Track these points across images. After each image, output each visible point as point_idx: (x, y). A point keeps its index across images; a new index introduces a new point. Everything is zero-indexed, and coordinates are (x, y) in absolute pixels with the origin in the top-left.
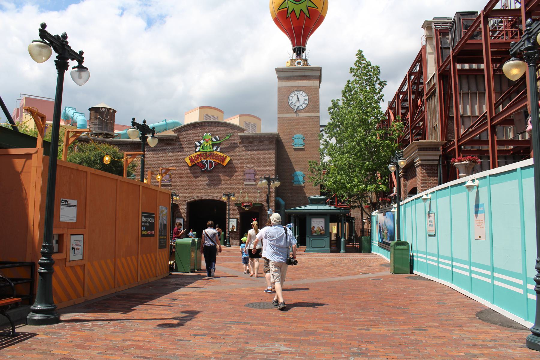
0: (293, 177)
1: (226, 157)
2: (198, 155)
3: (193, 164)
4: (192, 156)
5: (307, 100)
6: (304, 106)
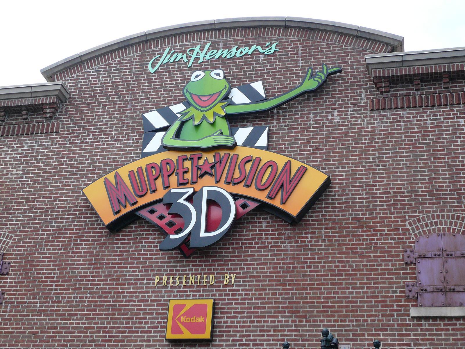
1: (302, 172)
2: (152, 166)
3: (124, 211)
4: (124, 172)
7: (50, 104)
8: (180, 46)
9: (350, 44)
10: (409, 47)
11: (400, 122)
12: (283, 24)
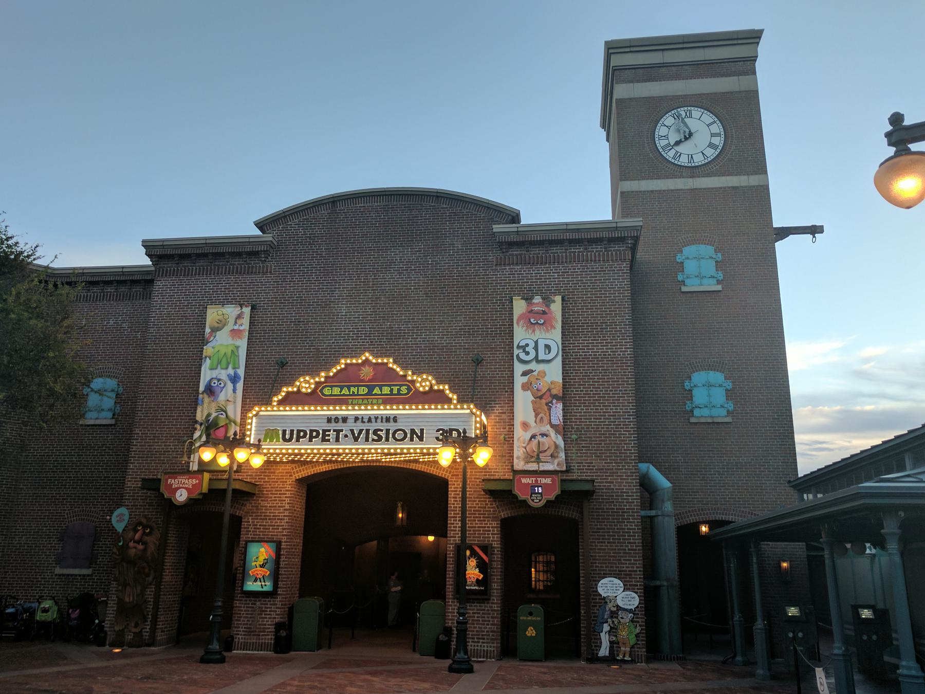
0: (690, 391)
5: (719, 135)
6: (711, 153)
7: (264, 251)
8: (360, 207)
9: (483, 213)
10: (524, 221)
11: (514, 274)
12: (435, 194)
